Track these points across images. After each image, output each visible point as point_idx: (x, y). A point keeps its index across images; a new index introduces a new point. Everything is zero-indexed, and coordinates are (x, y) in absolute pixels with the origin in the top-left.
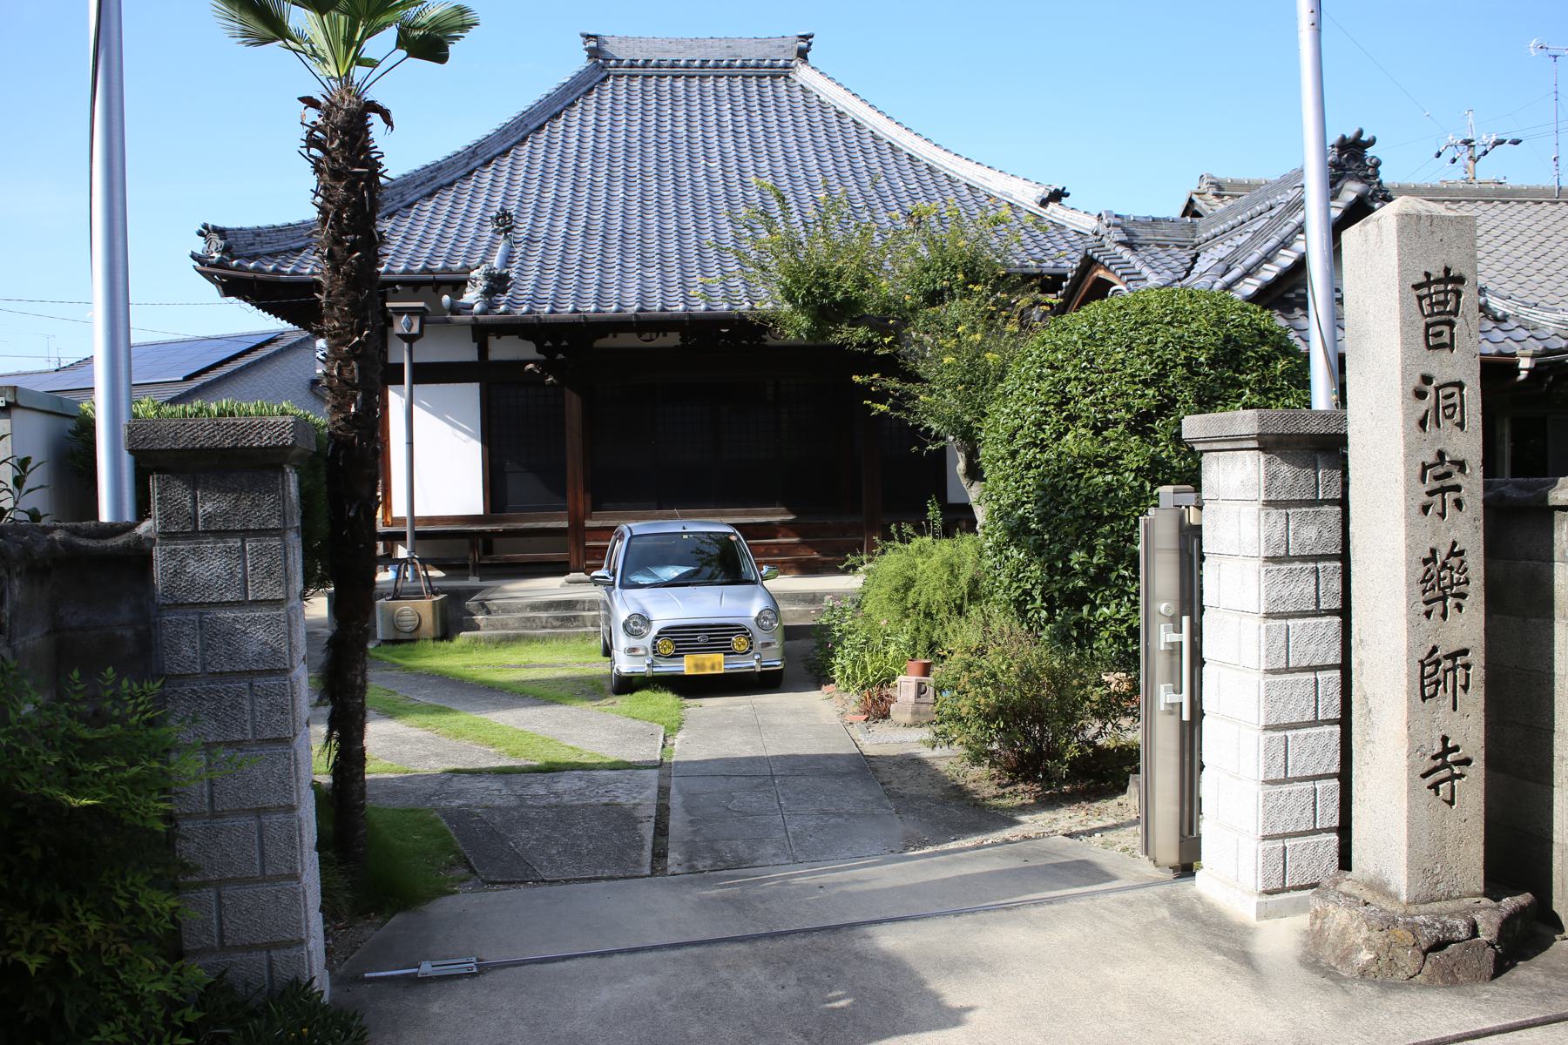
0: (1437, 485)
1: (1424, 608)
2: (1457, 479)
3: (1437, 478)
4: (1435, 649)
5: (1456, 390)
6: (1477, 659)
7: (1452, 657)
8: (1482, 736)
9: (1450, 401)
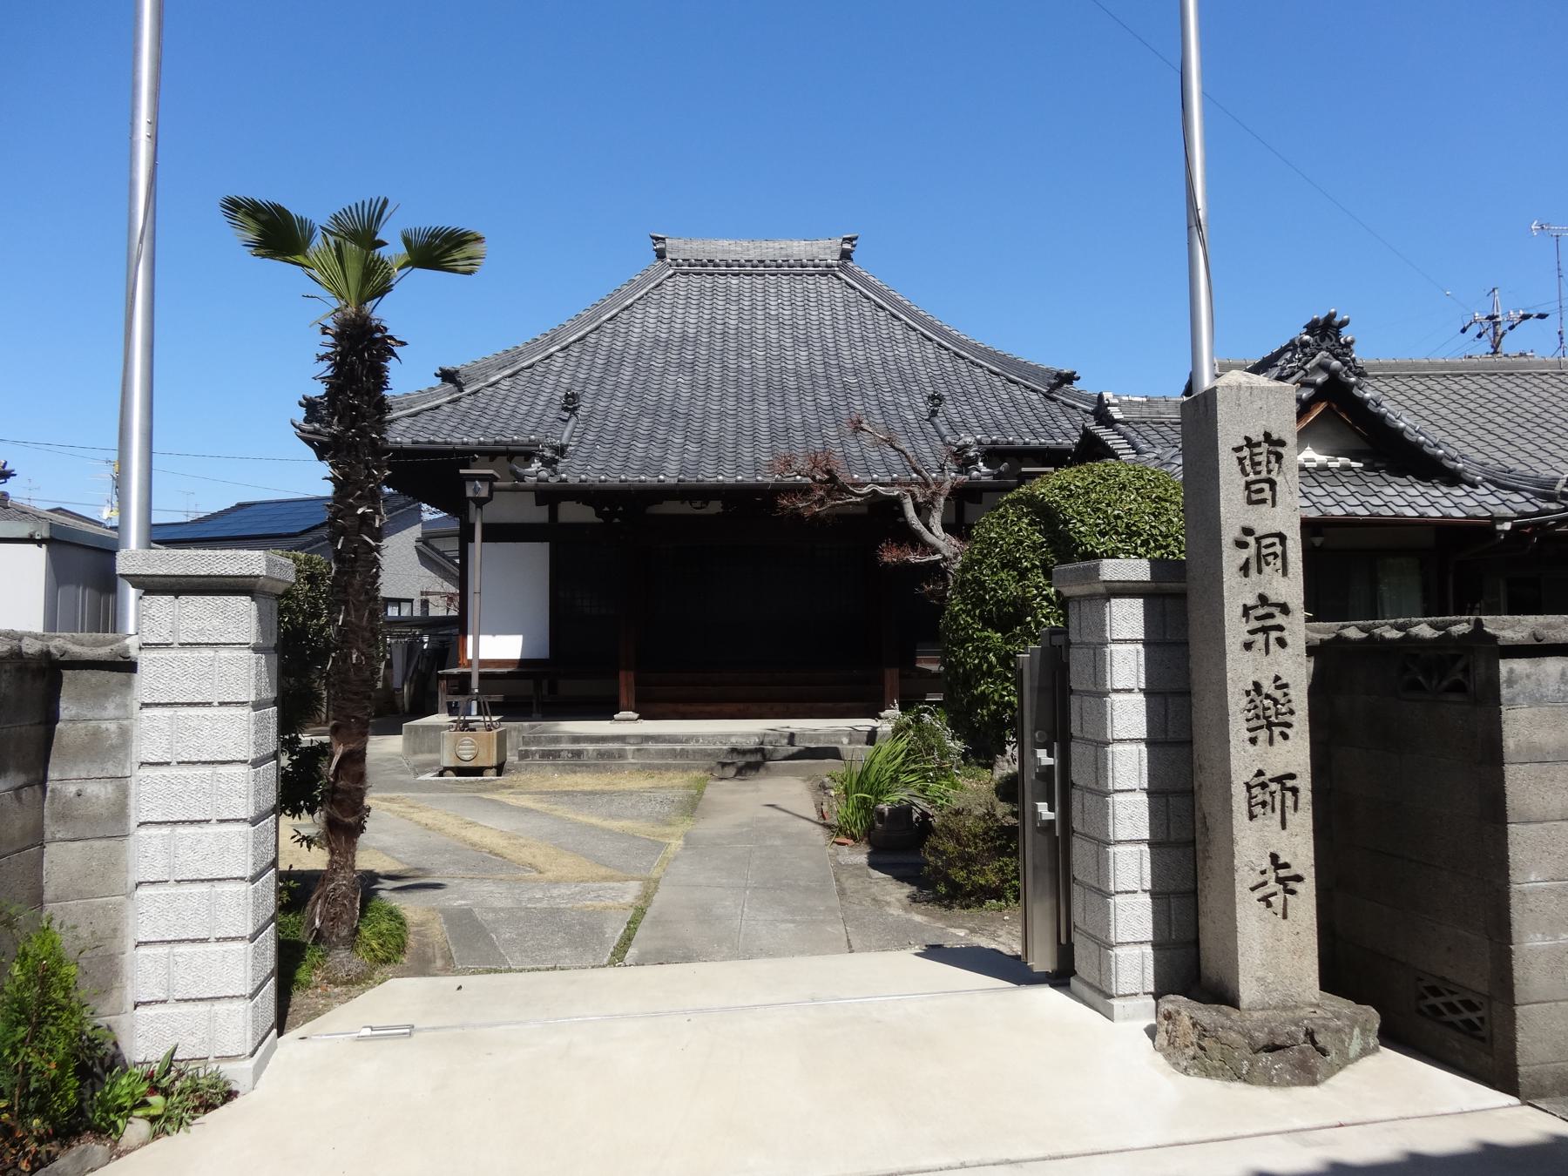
0: (1258, 624)
1: (1249, 735)
2: (1280, 619)
3: (1257, 618)
4: (1260, 773)
5: (1276, 540)
6: (1304, 783)
7: (1279, 780)
8: (1312, 855)
9: (1270, 550)
